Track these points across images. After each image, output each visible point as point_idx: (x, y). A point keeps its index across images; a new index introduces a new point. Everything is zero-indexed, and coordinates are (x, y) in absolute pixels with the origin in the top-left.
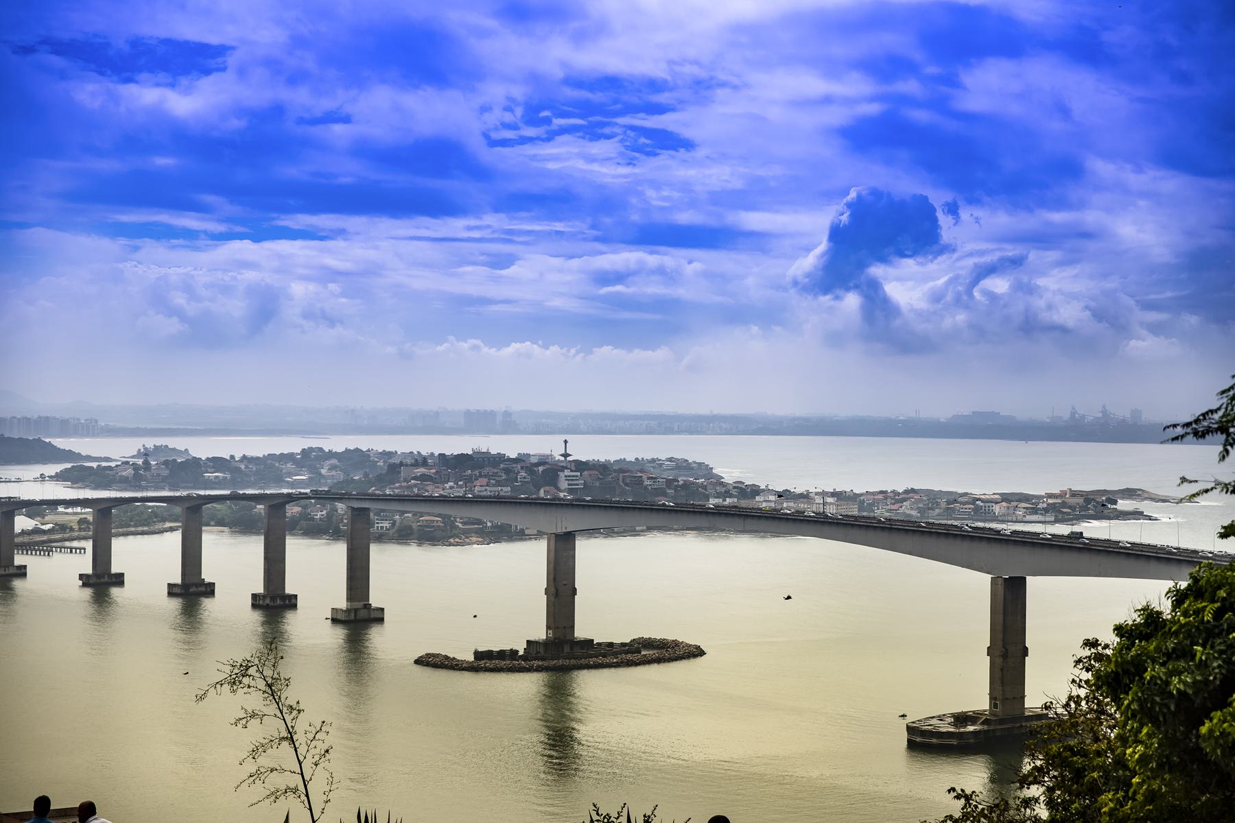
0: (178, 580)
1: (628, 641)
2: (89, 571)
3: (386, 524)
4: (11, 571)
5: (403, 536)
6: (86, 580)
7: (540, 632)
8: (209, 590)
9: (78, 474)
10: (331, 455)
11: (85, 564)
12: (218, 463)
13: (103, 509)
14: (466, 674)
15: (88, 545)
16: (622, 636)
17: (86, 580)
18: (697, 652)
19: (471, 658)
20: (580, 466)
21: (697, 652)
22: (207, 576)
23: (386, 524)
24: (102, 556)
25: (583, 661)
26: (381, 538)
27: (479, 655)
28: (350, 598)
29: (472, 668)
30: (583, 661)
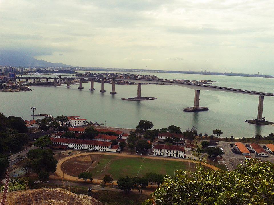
0: (90, 88)
3: (117, 82)
4: (69, 86)
5: (118, 83)
7: (137, 96)
8: (94, 89)
9: (78, 75)
10: (110, 74)
11: (79, 86)
12: (95, 74)
13: (81, 79)
19: (128, 99)
20: (141, 76)
22: (94, 88)
23: (117, 82)
24: (81, 85)
26: (116, 84)
27: (129, 98)
28: (112, 91)
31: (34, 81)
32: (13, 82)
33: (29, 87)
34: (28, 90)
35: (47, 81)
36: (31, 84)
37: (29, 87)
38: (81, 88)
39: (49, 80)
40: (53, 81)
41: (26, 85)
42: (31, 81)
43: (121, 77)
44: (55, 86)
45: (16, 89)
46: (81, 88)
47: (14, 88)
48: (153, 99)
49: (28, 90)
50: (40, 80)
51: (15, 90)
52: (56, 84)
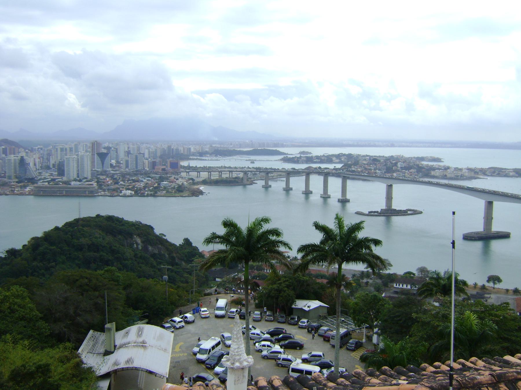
0: (304, 190)
1: (405, 209)
2: (285, 187)
4: (268, 186)
6: (284, 190)
11: (283, 185)
14: (366, 216)
15: (285, 179)
16: (404, 208)
17: (284, 190)
18: (421, 213)
21: (421, 213)
22: (311, 189)
25: (393, 214)
29: (367, 215)
30: (393, 214)
31: (210, 176)
32: (177, 179)
33: (202, 188)
34: (201, 193)
35: (231, 177)
36: (205, 182)
37: (202, 188)
38: (288, 189)
39: (235, 175)
40: (241, 175)
41: (198, 183)
42: (204, 175)
43: (365, 164)
44: (244, 185)
45: (182, 191)
46: (288, 190)
47: (180, 190)
48: (415, 212)
49: (201, 193)
50: (231, 175)
51: (181, 194)
52: (245, 181)
